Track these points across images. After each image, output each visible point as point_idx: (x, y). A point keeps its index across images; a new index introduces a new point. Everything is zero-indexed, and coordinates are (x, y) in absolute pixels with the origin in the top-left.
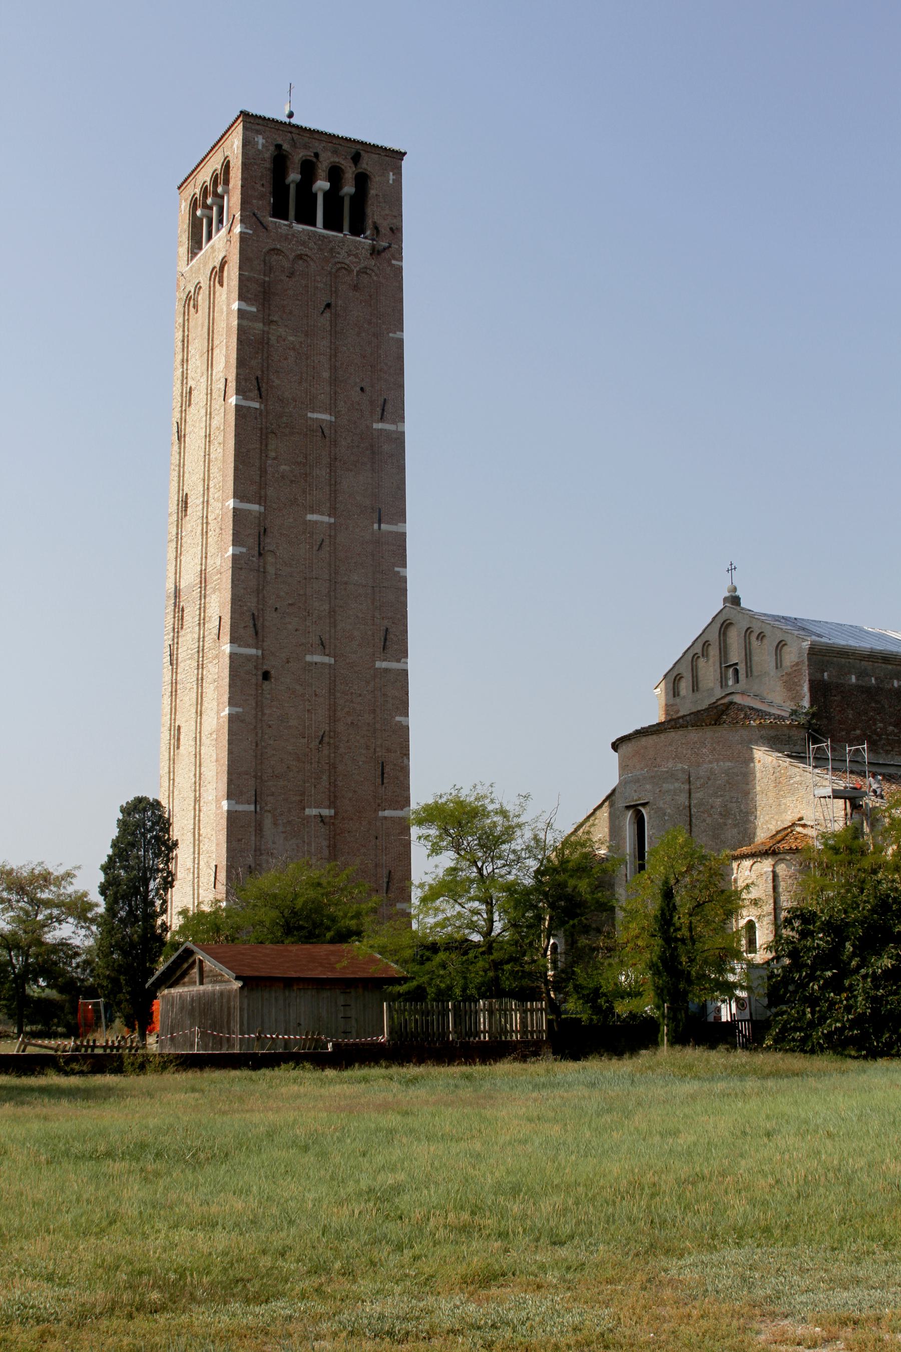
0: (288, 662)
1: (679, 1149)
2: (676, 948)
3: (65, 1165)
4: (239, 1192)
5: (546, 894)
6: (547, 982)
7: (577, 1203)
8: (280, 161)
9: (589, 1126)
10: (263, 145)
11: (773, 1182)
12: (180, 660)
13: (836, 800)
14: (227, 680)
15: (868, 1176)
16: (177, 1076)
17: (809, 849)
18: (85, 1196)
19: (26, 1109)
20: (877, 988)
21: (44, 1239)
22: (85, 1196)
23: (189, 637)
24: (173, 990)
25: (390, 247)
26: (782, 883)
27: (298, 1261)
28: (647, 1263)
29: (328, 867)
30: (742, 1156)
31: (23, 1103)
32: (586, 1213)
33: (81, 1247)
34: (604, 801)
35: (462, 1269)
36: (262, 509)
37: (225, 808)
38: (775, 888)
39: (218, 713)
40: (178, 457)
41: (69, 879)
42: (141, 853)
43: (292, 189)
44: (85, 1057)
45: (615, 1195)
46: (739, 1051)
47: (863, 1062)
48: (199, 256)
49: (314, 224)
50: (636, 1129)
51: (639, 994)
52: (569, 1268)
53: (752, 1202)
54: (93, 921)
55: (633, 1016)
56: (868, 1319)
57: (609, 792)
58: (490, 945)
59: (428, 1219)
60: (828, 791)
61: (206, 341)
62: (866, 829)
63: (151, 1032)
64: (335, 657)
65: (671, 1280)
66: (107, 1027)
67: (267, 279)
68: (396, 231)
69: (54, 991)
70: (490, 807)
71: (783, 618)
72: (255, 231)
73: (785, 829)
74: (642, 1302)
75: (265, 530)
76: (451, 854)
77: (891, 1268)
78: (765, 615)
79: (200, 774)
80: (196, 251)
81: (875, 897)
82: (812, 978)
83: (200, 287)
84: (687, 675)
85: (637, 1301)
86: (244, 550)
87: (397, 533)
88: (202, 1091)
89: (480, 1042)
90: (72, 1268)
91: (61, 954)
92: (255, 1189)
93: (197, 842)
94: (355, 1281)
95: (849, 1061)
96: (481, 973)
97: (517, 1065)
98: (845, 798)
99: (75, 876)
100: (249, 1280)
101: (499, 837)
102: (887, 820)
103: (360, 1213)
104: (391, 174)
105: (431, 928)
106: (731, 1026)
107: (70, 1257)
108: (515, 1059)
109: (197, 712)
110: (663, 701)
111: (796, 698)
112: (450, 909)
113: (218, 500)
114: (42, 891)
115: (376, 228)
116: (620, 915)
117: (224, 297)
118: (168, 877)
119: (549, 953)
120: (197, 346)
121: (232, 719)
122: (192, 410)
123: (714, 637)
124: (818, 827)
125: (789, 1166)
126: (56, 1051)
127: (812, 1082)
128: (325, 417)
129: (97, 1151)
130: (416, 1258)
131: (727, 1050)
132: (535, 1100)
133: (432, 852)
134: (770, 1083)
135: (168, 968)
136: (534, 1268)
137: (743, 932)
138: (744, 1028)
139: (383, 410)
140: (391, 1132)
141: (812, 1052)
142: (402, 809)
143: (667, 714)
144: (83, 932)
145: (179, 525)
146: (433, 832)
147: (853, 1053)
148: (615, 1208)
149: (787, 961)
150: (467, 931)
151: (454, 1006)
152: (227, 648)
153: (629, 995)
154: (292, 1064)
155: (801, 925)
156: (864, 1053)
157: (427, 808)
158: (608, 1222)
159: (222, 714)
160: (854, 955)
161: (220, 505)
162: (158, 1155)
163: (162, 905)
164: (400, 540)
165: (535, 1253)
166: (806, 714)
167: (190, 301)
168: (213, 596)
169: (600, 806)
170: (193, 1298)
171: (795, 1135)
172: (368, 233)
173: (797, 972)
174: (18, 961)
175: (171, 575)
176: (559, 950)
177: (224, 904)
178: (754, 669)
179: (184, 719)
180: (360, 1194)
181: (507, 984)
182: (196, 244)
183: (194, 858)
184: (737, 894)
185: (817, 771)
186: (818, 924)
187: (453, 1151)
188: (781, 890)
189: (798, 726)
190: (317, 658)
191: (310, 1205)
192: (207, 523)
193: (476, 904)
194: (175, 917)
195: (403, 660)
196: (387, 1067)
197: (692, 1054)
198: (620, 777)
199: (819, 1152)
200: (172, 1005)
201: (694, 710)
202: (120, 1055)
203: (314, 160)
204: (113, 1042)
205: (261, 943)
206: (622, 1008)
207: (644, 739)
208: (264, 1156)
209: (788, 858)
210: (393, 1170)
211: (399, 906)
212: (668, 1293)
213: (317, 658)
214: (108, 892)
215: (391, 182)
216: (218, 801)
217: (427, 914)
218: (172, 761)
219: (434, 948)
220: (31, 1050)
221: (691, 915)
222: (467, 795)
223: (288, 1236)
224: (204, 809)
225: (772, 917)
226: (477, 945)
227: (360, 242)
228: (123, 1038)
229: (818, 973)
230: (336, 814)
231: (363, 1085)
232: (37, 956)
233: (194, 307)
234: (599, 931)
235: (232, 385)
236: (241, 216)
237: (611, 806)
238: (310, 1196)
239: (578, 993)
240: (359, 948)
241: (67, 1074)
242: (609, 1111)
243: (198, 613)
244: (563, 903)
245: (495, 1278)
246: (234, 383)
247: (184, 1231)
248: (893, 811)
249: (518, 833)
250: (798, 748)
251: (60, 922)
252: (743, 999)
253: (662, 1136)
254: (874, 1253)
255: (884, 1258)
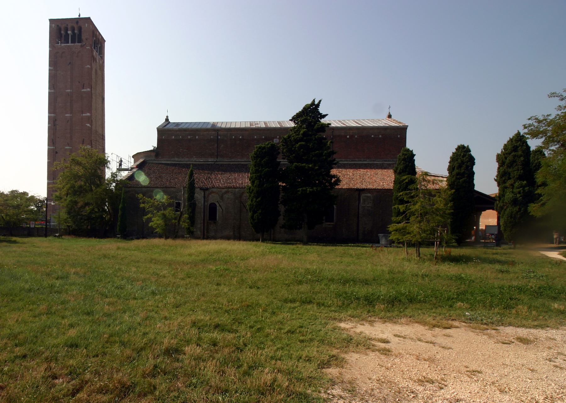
8: (60, 29)
75: (56, 120)
128: (69, 91)
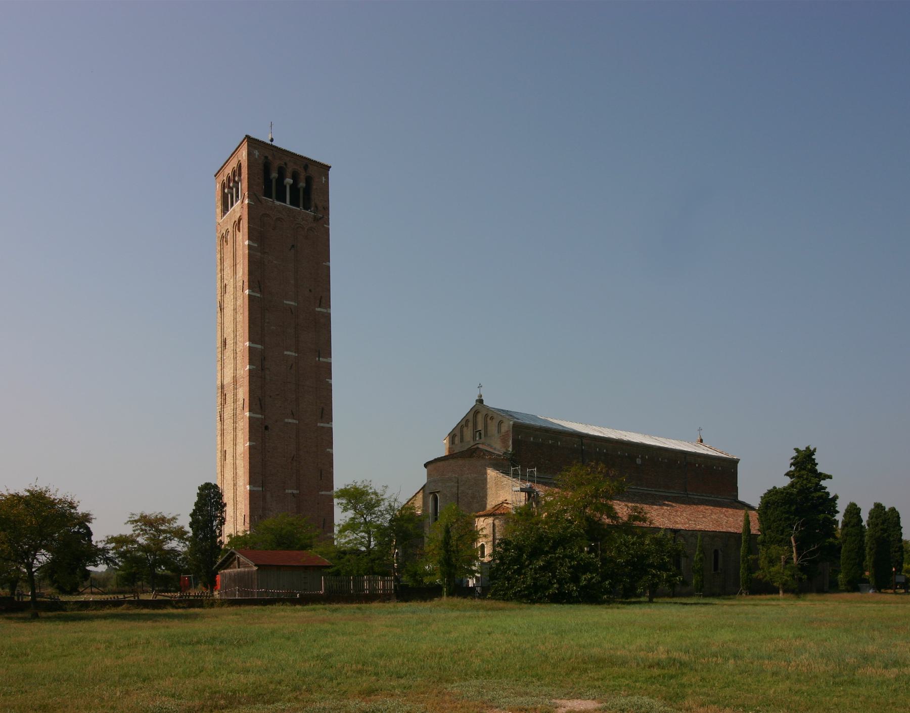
0: (276, 422)
1: (451, 639)
2: (450, 555)
3: (178, 647)
4: (258, 657)
5: (394, 530)
6: (394, 568)
7: (408, 661)
9: (413, 629)
10: (258, 156)
11: (491, 653)
12: (225, 419)
13: (521, 493)
14: (248, 429)
15: (531, 651)
16: (228, 608)
17: (509, 513)
18: (188, 660)
19: (158, 624)
20: (536, 574)
21: (169, 679)
22: (188, 660)
23: (229, 408)
24: (225, 571)
25: (323, 217)
26: (497, 528)
27: (287, 686)
28: (438, 686)
29: (296, 516)
30: (478, 642)
31: (156, 621)
32: (412, 665)
33: (187, 682)
34: (420, 490)
35: (358, 688)
36: (263, 347)
37: (248, 489)
38: (494, 530)
39: (244, 445)
40: (220, 319)
41: (174, 520)
42: (209, 508)
43: (274, 181)
44: (185, 600)
45: (424, 657)
46: (477, 599)
47: (529, 605)
48: (227, 214)
49: (285, 202)
50: (433, 631)
51: (435, 574)
52: (405, 687)
53: (483, 661)
54: (186, 539)
55: (431, 583)
56: (531, 709)
57: (422, 486)
58: (369, 551)
59: (344, 668)
60: (518, 489)
61: (232, 260)
62: (534, 506)
63: (215, 589)
64: (298, 420)
65: (448, 692)
66: (195, 587)
67: (262, 230)
68: (326, 209)
69: (169, 572)
70: (370, 491)
71: (502, 410)
72: (255, 203)
73: (499, 504)
74: (436, 701)
75: (264, 358)
76: (352, 511)
77: (540, 688)
78: (494, 408)
79: (236, 473)
80: (225, 211)
81: (537, 535)
82: (509, 569)
83: (228, 232)
84: (459, 435)
85: (434, 701)
86: (254, 367)
87: (327, 362)
88: (240, 615)
89: (365, 594)
90: (183, 691)
91: (172, 555)
92: (266, 656)
93: (235, 504)
94: (312, 694)
95: (523, 604)
96: (366, 564)
97: (381, 604)
98: (526, 492)
99: (177, 519)
100: (265, 695)
101: (374, 504)
102: (543, 502)
103: (314, 665)
104: (323, 178)
105: (343, 544)
106: (473, 588)
107: (182, 687)
108: (380, 602)
109: (234, 444)
110: (448, 446)
111: (507, 447)
112: (352, 536)
113: (241, 342)
114: (162, 526)
115: (316, 207)
116: (426, 540)
117: (241, 237)
118: (222, 519)
119: (395, 556)
120: (228, 263)
121: (250, 447)
122: (227, 296)
123: (471, 417)
124: (513, 504)
125: (498, 646)
126: (171, 598)
127: (507, 613)
129: (192, 641)
130: (338, 684)
131: (471, 598)
132: (389, 619)
133: (344, 510)
134: (490, 613)
135: (223, 561)
136: (390, 688)
137: (479, 549)
138: (478, 589)
139: (320, 301)
140: (326, 632)
141: (508, 600)
142: (330, 491)
143: (449, 452)
144: (182, 544)
145: (222, 353)
146: (344, 501)
147: (525, 601)
148: (424, 663)
149: (498, 561)
150: (359, 546)
151: (353, 578)
152: (247, 414)
153: (430, 575)
154: (281, 603)
155: (505, 546)
156: (529, 601)
157: (341, 491)
158: (421, 669)
159: (246, 445)
160: (527, 559)
161: (242, 344)
162: (222, 642)
163: (220, 532)
164: (329, 366)
165: (390, 681)
166: (510, 454)
167: (224, 238)
168: (240, 389)
169: (418, 492)
170: (240, 702)
171: (501, 634)
172: (312, 209)
173: (503, 566)
174: (151, 558)
175: (219, 377)
176: (399, 555)
177: (248, 533)
178: (488, 432)
179: (228, 447)
180: (313, 657)
181: (376, 569)
182: (225, 209)
183: (234, 512)
184: (477, 532)
185: (514, 479)
186: (512, 546)
187: (354, 639)
188: (496, 531)
189: (506, 460)
190: (290, 421)
191: (292, 662)
192: (236, 353)
193: (363, 534)
194: (226, 538)
195: (330, 423)
196: (324, 604)
197: (456, 600)
198: (427, 479)
199: (511, 641)
200: (226, 577)
201: (460, 451)
202: (202, 600)
203: (285, 166)
204: (198, 594)
205: (266, 550)
206: (427, 580)
207: (439, 463)
208: (270, 642)
209: (500, 517)
210: (328, 647)
211: (329, 534)
212: (447, 698)
213: (290, 421)
214: (194, 526)
215: (323, 182)
216: (245, 485)
217: (341, 538)
218: (223, 466)
219: (344, 553)
220: (159, 598)
221: (457, 541)
222: (359, 485)
223: (282, 675)
224: (238, 489)
225: (492, 543)
226: (364, 552)
227: (309, 214)
228: (203, 592)
229: (511, 567)
230: (300, 492)
231: (313, 612)
232: (160, 555)
233: (226, 242)
234: (417, 547)
235: (246, 284)
236: (248, 194)
237: (423, 492)
238: (291, 659)
239: (407, 573)
240: (311, 552)
241: (177, 608)
242: (421, 623)
243: (233, 396)
244: (401, 534)
245: (373, 692)
246: (247, 283)
247: (234, 674)
248: (546, 498)
249: (382, 503)
250: (506, 469)
251: (171, 540)
252: (479, 577)
253: (444, 633)
254: (534, 682)
255: (538, 684)
